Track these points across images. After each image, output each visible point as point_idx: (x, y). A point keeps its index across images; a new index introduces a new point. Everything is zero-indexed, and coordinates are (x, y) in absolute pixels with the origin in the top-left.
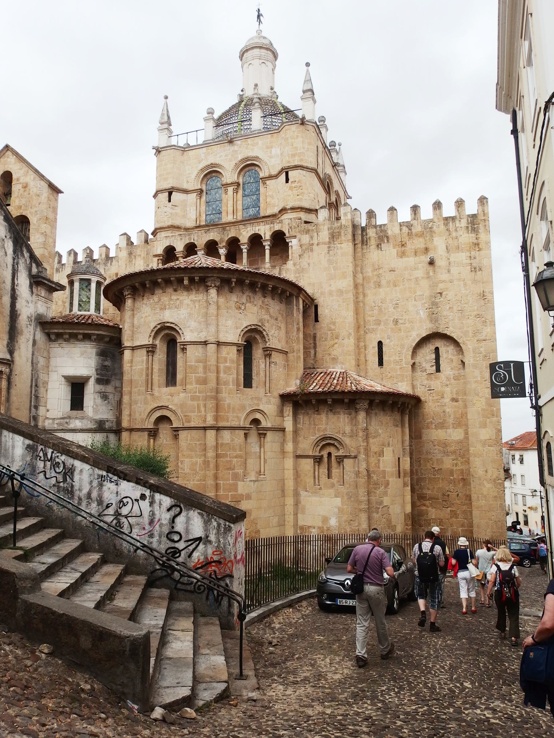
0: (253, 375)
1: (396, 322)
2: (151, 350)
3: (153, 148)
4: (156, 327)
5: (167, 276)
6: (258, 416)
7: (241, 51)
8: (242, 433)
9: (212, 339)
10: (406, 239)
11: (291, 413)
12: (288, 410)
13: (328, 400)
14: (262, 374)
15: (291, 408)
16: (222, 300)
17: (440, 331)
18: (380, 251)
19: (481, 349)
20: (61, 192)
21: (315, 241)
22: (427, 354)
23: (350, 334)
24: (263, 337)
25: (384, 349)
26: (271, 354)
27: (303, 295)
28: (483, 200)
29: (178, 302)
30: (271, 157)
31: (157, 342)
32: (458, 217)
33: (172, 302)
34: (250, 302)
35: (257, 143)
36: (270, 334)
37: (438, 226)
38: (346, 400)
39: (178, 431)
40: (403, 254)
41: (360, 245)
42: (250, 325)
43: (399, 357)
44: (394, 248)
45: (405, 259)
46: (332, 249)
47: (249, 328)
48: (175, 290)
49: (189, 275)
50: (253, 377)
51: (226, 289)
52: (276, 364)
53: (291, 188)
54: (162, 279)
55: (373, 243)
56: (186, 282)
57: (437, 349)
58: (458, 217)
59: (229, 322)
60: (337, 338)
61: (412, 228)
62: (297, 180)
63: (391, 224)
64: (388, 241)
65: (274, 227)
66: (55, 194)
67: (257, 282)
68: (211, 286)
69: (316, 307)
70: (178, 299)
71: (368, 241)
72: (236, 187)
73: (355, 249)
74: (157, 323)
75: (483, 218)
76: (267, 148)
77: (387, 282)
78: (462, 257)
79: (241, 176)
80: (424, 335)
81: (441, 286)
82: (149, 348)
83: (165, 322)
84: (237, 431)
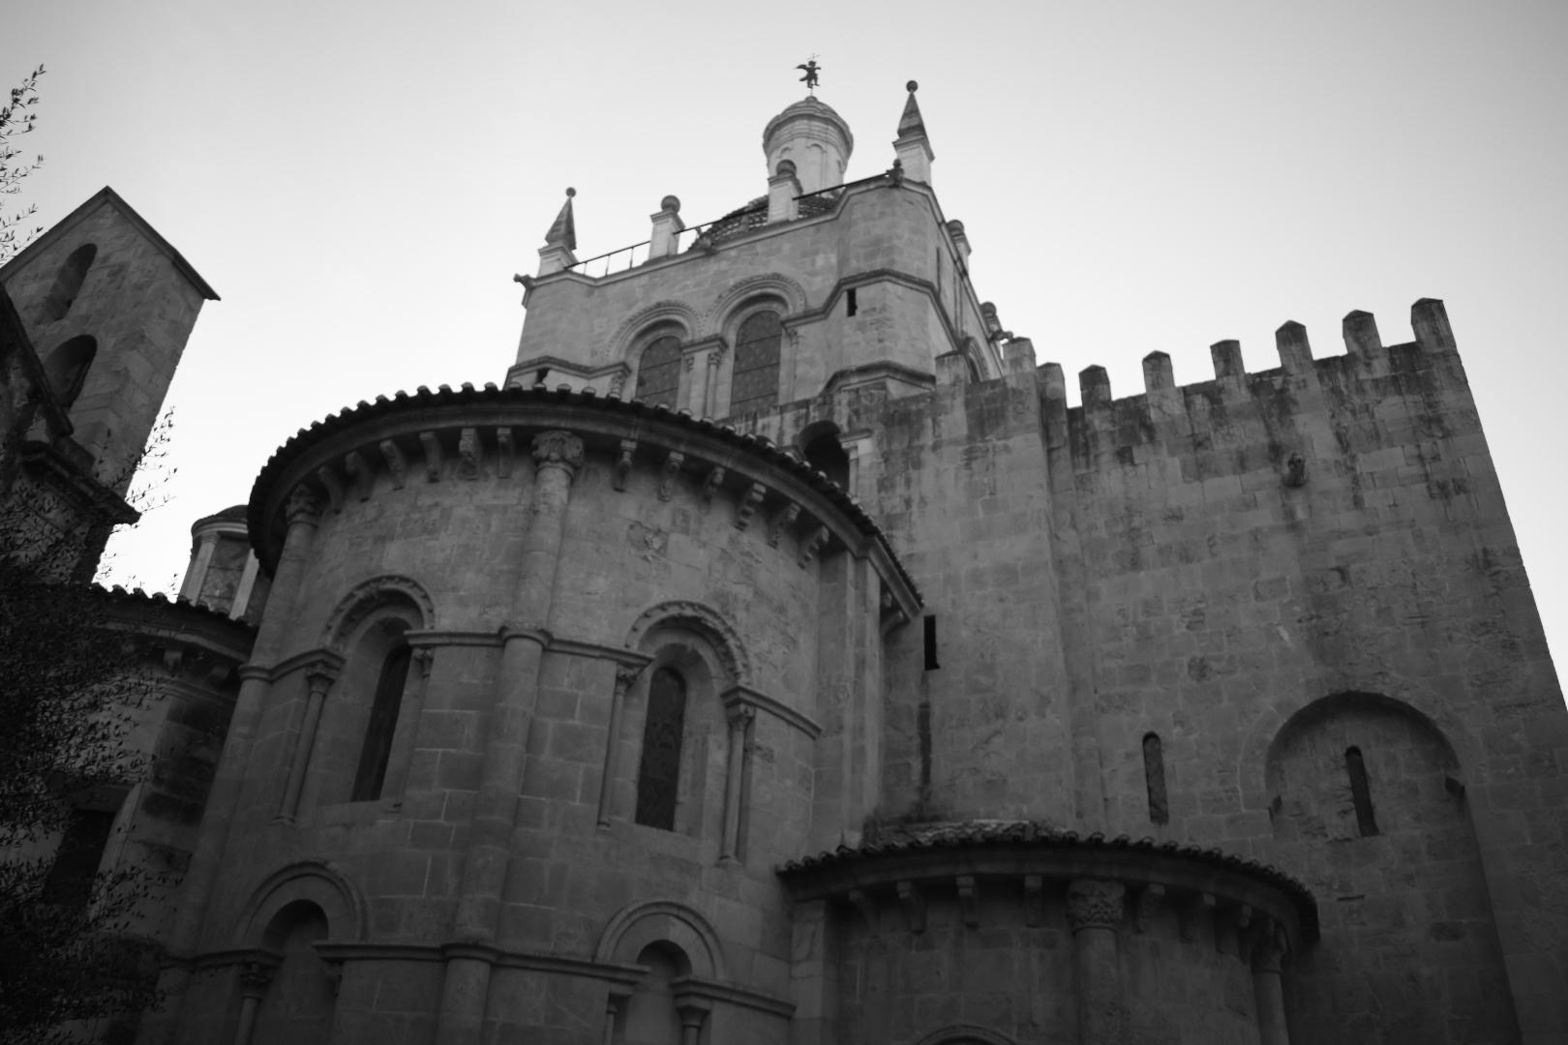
0: (681, 788)
1: (1200, 669)
2: (320, 671)
3: (518, 279)
4: (351, 596)
5: (405, 429)
6: (678, 933)
7: (767, 129)
8: (599, 991)
9: (525, 623)
10: (1206, 428)
11: (819, 948)
12: (813, 930)
13: (961, 881)
14: (713, 784)
15: (821, 926)
16: (581, 511)
17: (1357, 685)
18: (1128, 468)
19: (1516, 736)
20: (214, 296)
21: (928, 439)
22: (1322, 757)
23: (1045, 701)
24: (727, 657)
25: (1168, 759)
26: (751, 720)
27: (882, 559)
28: (1428, 312)
29: (436, 514)
30: (813, 274)
31: (349, 651)
32: (1360, 354)
33: (416, 516)
34: (686, 531)
35: (779, 250)
36: (752, 650)
37: (1303, 385)
38: (1032, 883)
39: (340, 962)
40: (1200, 470)
41: (1066, 452)
42: (678, 604)
43: (1223, 782)
44: (1172, 454)
45: (1211, 482)
46: (979, 454)
47: (674, 611)
48: (433, 479)
49: (479, 422)
50: (681, 798)
51: (605, 476)
52: (768, 756)
53: (861, 327)
54: (396, 440)
55: (1106, 448)
56: (467, 442)
57: (1353, 752)
58: (1360, 354)
59: (601, 581)
60: (1000, 714)
61: (1223, 396)
62: (878, 306)
63: (1158, 392)
64: (1151, 438)
65: (807, 415)
66: (192, 295)
67: (711, 466)
68: (548, 459)
69: (930, 623)
70: (436, 505)
71: (1091, 444)
72: (717, 350)
73: (1050, 463)
74: (356, 584)
75: (1440, 350)
76: (804, 255)
77: (1160, 551)
78: (1395, 458)
79: (732, 327)
80: (1303, 701)
81: (1340, 547)
82: (313, 665)
83: (378, 580)
84: (580, 983)
